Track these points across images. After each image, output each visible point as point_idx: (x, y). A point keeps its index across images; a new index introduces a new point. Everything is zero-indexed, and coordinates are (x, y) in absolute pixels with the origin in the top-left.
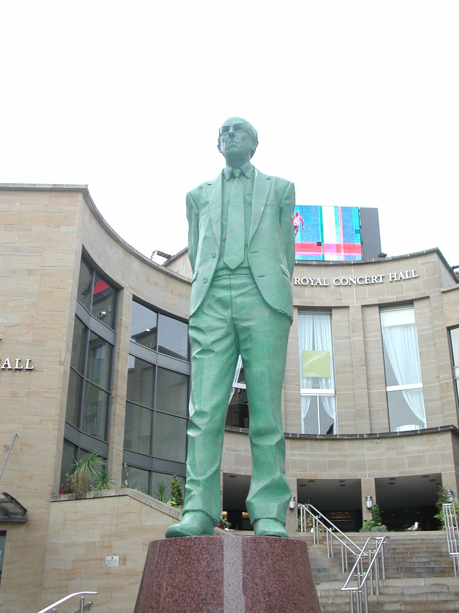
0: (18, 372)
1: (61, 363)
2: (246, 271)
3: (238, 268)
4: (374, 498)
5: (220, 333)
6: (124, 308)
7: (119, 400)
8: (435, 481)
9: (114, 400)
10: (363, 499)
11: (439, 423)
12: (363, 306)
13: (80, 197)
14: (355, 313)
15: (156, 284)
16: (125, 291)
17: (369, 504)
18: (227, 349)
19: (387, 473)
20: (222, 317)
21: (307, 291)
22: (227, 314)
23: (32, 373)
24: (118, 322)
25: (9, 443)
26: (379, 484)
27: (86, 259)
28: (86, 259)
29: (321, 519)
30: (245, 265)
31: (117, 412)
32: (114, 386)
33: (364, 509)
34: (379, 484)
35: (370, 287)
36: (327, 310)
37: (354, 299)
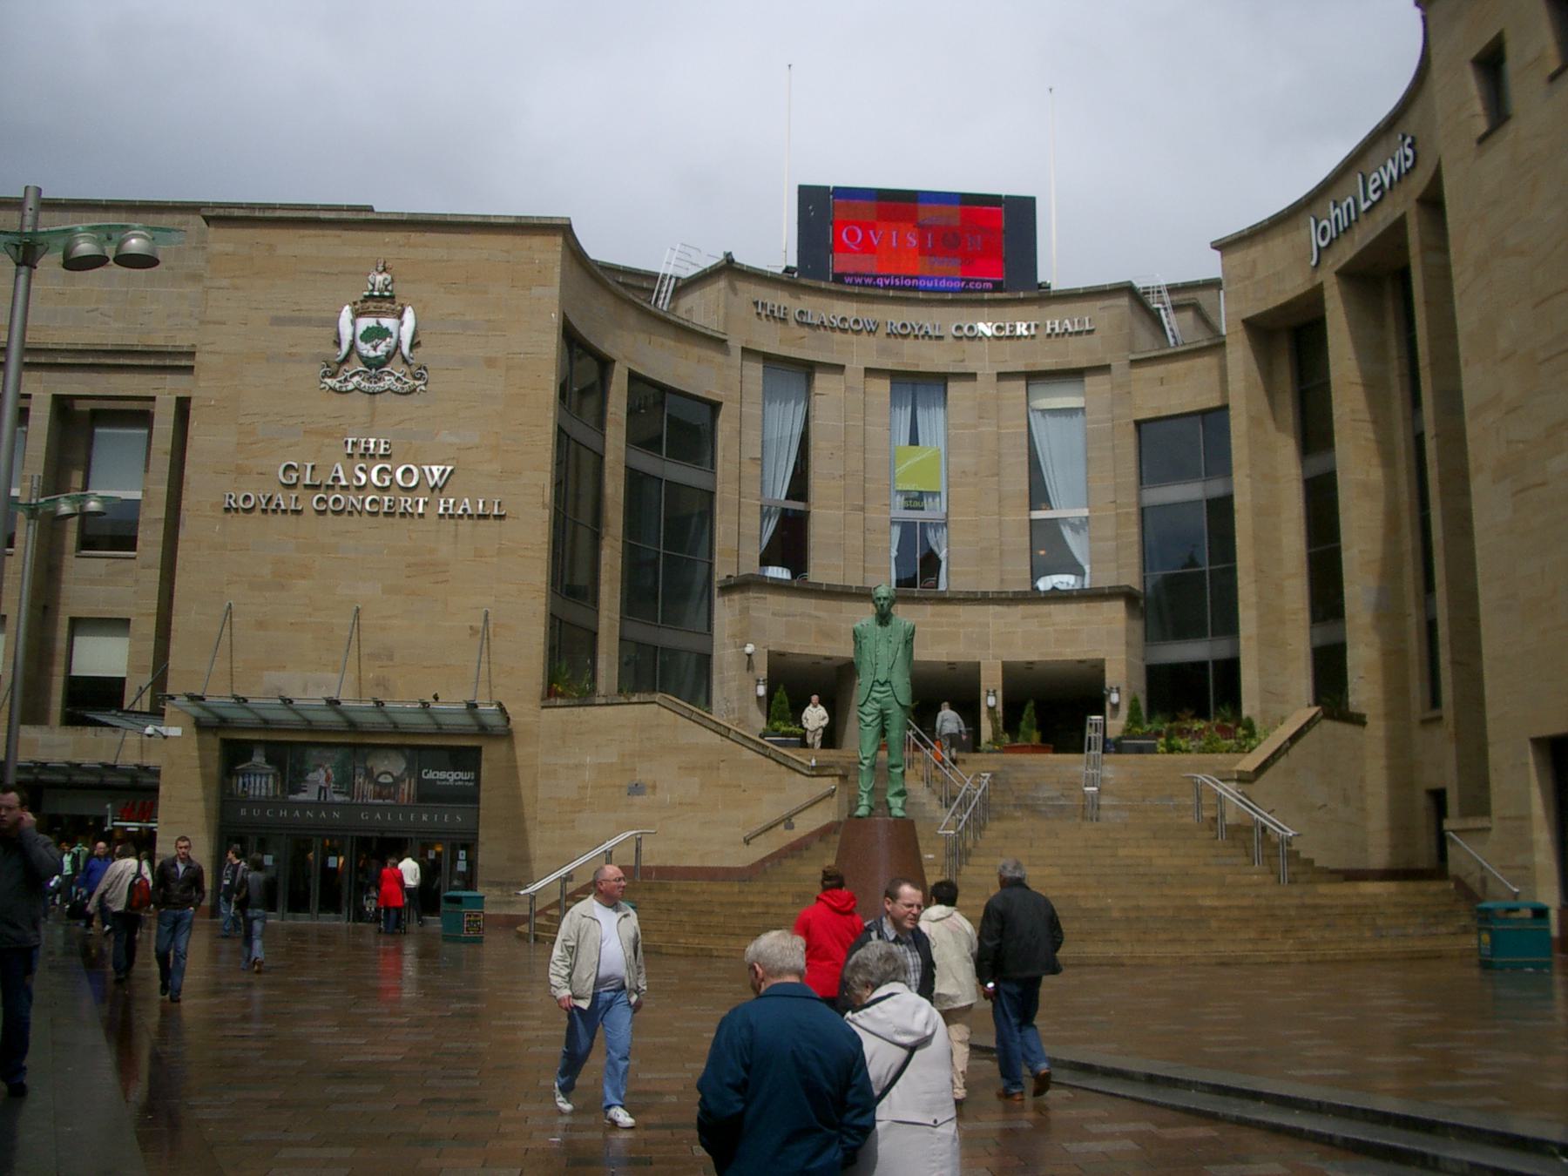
0: (482, 522)
4: (1000, 693)
8: (1098, 668)
10: (983, 693)
11: (1107, 580)
12: (999, 374)
16: (617, 366)
17: (991, 701)
26: (1009, 670)
33: (984, 709)
34: (1009, 670)
35: (1014, 342)
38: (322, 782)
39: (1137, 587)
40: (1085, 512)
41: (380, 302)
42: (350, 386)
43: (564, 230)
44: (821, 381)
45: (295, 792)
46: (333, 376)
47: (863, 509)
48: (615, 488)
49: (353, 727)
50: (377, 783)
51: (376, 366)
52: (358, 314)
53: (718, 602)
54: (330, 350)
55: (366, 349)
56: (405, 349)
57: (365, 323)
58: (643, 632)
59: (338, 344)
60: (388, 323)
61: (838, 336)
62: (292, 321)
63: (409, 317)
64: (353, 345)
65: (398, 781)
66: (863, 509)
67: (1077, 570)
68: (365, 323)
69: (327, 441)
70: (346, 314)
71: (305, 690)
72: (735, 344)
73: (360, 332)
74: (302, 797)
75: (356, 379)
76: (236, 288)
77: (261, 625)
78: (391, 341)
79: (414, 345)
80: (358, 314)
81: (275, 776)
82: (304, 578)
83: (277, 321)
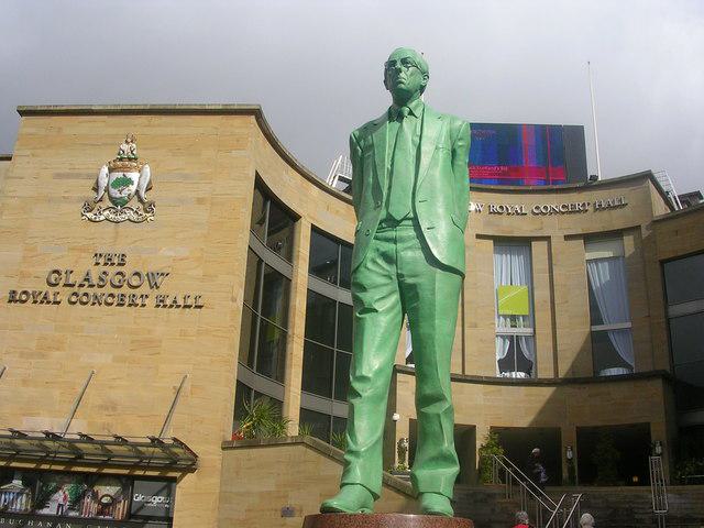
1: (234, 300)
2: (410, 222)
3: (405, 218)
4: (575, 445)
5: (385, 290)
6: (302, 241)
9: (289, 339)
10: (563, 450)
13: (252, 119)
16: (303, 220)
17: (569, 455)
18: (392, 308)
19: (590, 421)
20: (385, 273)
22: (392, 270)
28: (260, 185)
29: (515, 472)
30: (412, 215)
31: (295, 352)
32: (290, 324)
33: (564, 460)
38: (61, 501)
39: (668, 368)
40: (628, 325)
41: (123, 162)
42: (102, 218)
43: (257, 113)
45: (42, 507)
46: (91, 211)
48: (299, 304)
49: (79, 457)
50: (100, 503)
55: (115, 193)
58: (320, 404)
59: (96, 189)
60: (134, 176)
62: (68, 176)
63: (147, 169)
64: (107, 190)
65: (114, 501)
67: (620, 363)
69: (83, 255)
70: (105, 170)
74: (45, 511)
77: (25, 382)
78: (133, 188)
79: (148, 189)
80: (111, 170)
81: (28, 495)
82: (58, 349)
83: (59, 176)
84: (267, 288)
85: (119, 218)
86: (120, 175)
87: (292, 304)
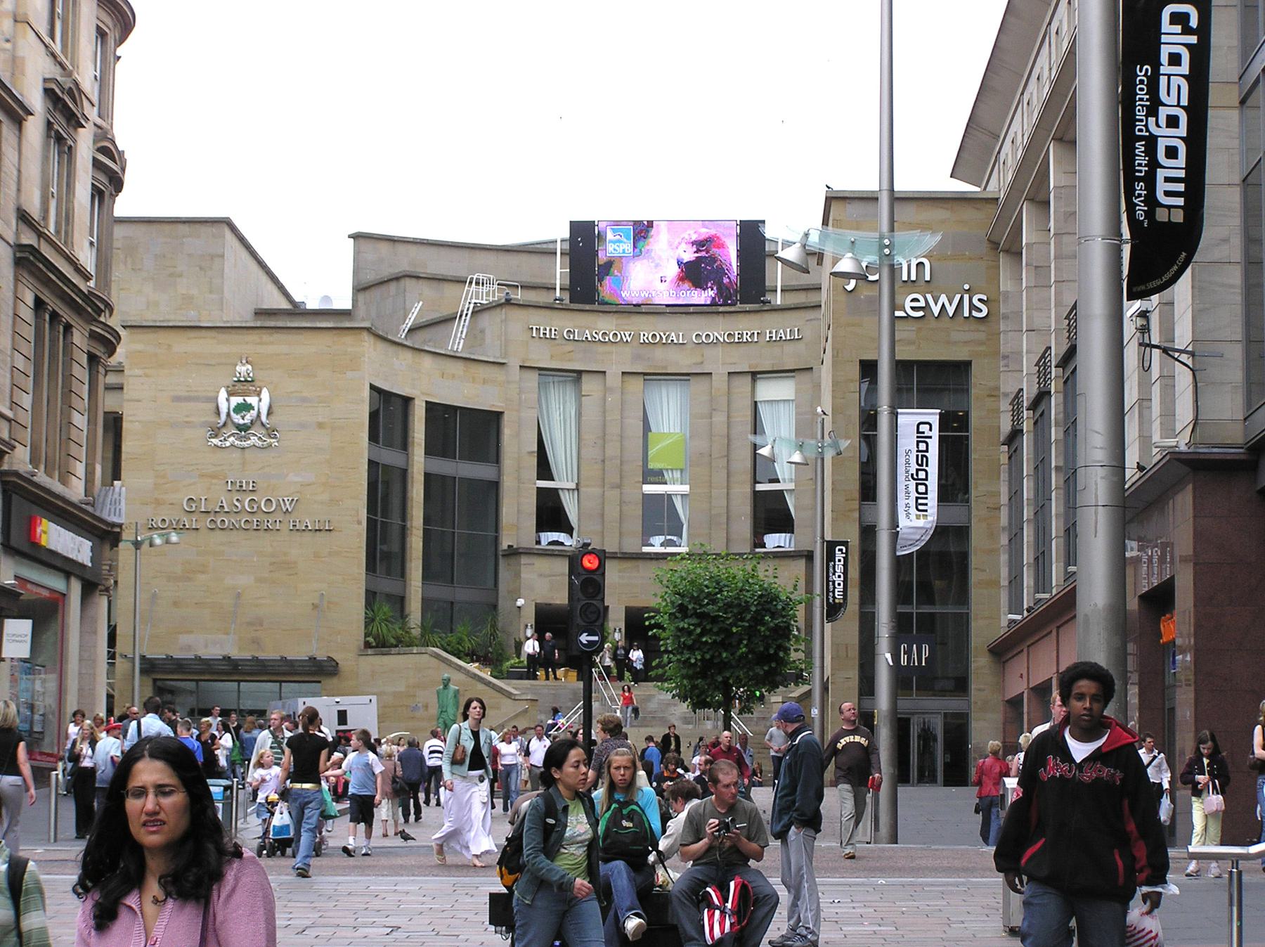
1: (359, 523)
7: (414, 531)
14: (719, 381)
15: (453, 376)
16: (417, 402)
21: (659, 353)
23: (333, 533)
24: (410, 439)
25: (316, 602)
27: (372, 387)
35: (742, 348)
36: (684, 376)
37: (719, 364)
41: (243, 386)
42: (228, 444)
44: (588, 384)
46: (216, 436)
47: (619, 486)
48: (417, 492)
51: (242, 428)
52: (231, 394)
53: (502, 563)
54: (212, 419)
55: (237, 419)
56: (264, 418)
57: (236, 400)
58: (442, 592)
59: (218, 413)
60: (252, 400)
61: (601, 348)
62: (188, 399)
63: (265, 394)
64: (228, 414)
66: (619, 486)
68: (236, 400)
70: (223, 395)
71: (206, 646)
72: (514, 363)
73: (232, 407)
75: (232, 439)
76: (147, 376)
78: (254, 413)
79: (269, 413)
80: (230, 394)
82: (203, 572)
83: (177, 399)
84: (384, 488)
85: (245, 444)
86: (240, 400)
87: (409, 495)
